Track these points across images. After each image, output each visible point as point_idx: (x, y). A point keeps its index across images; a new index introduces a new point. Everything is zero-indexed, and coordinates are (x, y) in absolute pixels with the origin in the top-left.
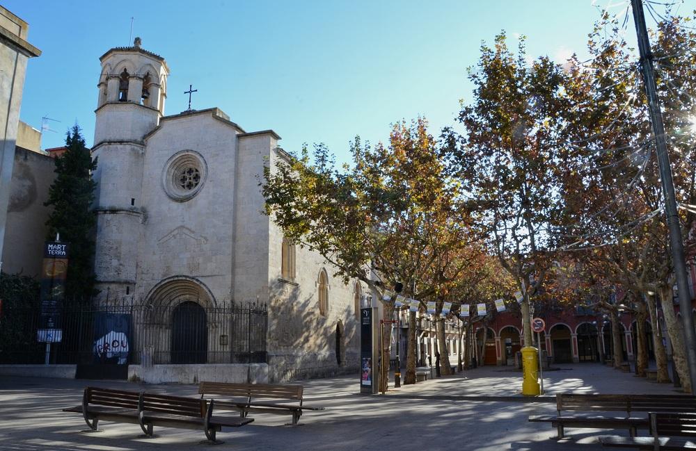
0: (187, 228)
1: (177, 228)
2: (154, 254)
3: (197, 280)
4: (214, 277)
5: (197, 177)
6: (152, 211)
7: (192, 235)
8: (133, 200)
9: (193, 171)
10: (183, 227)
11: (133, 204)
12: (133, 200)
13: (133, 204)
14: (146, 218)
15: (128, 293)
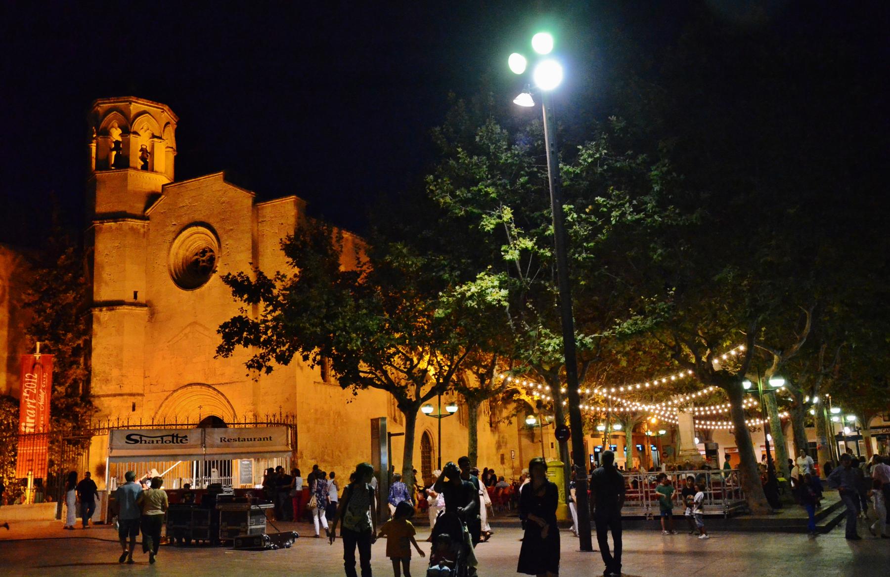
0: (201, 325)
1: (190, 324)
2: (164, 358)
3: (215, 389)
4: (233, 385)
5: (212, 260)
6: (160, 306)
7: (207, 333)
8: (135, 293)
9: (206, 252)
10: (195, 323)
11: (135, 297)
12: (135, 293)
13: (135, 297)
14: (152, 314)
15: (134, 409)
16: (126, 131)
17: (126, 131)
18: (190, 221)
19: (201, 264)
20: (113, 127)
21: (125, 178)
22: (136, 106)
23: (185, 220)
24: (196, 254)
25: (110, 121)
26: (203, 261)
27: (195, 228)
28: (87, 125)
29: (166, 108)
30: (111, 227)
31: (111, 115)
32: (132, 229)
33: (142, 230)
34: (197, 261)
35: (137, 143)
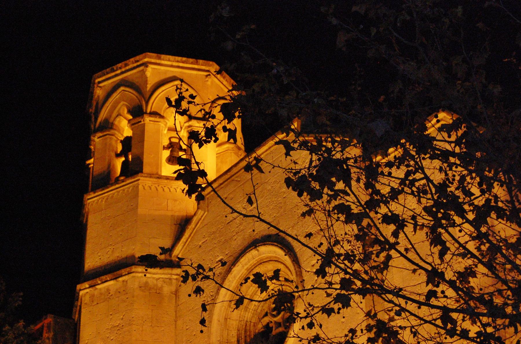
16: (137, 112)
17: (137, 112)
18: (246, 243)
19: (274, 332)
20: (119, 115)
21: (135, 194)
22: (158, 68)
23: (238, 243)
24: (266, 315)
25: (114, 107)
26: (278, 324)
27: (254, 252)
28: (81, 123)
29: (214, 67)
30: (108, 290)
31: (116, 96)
32: (145, 287)
33: (167, 290)
34: (268, 328)
35: (158, 132)
